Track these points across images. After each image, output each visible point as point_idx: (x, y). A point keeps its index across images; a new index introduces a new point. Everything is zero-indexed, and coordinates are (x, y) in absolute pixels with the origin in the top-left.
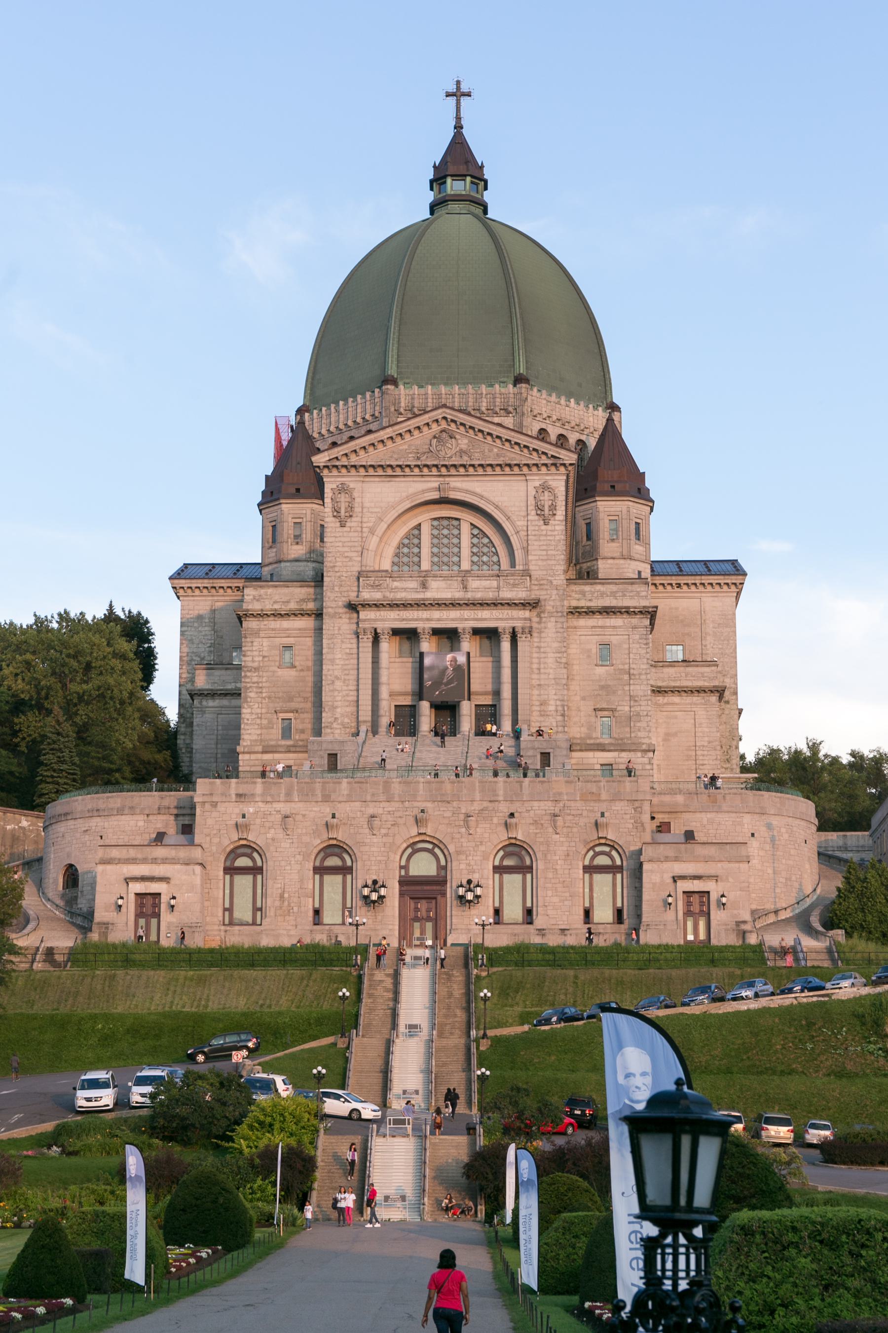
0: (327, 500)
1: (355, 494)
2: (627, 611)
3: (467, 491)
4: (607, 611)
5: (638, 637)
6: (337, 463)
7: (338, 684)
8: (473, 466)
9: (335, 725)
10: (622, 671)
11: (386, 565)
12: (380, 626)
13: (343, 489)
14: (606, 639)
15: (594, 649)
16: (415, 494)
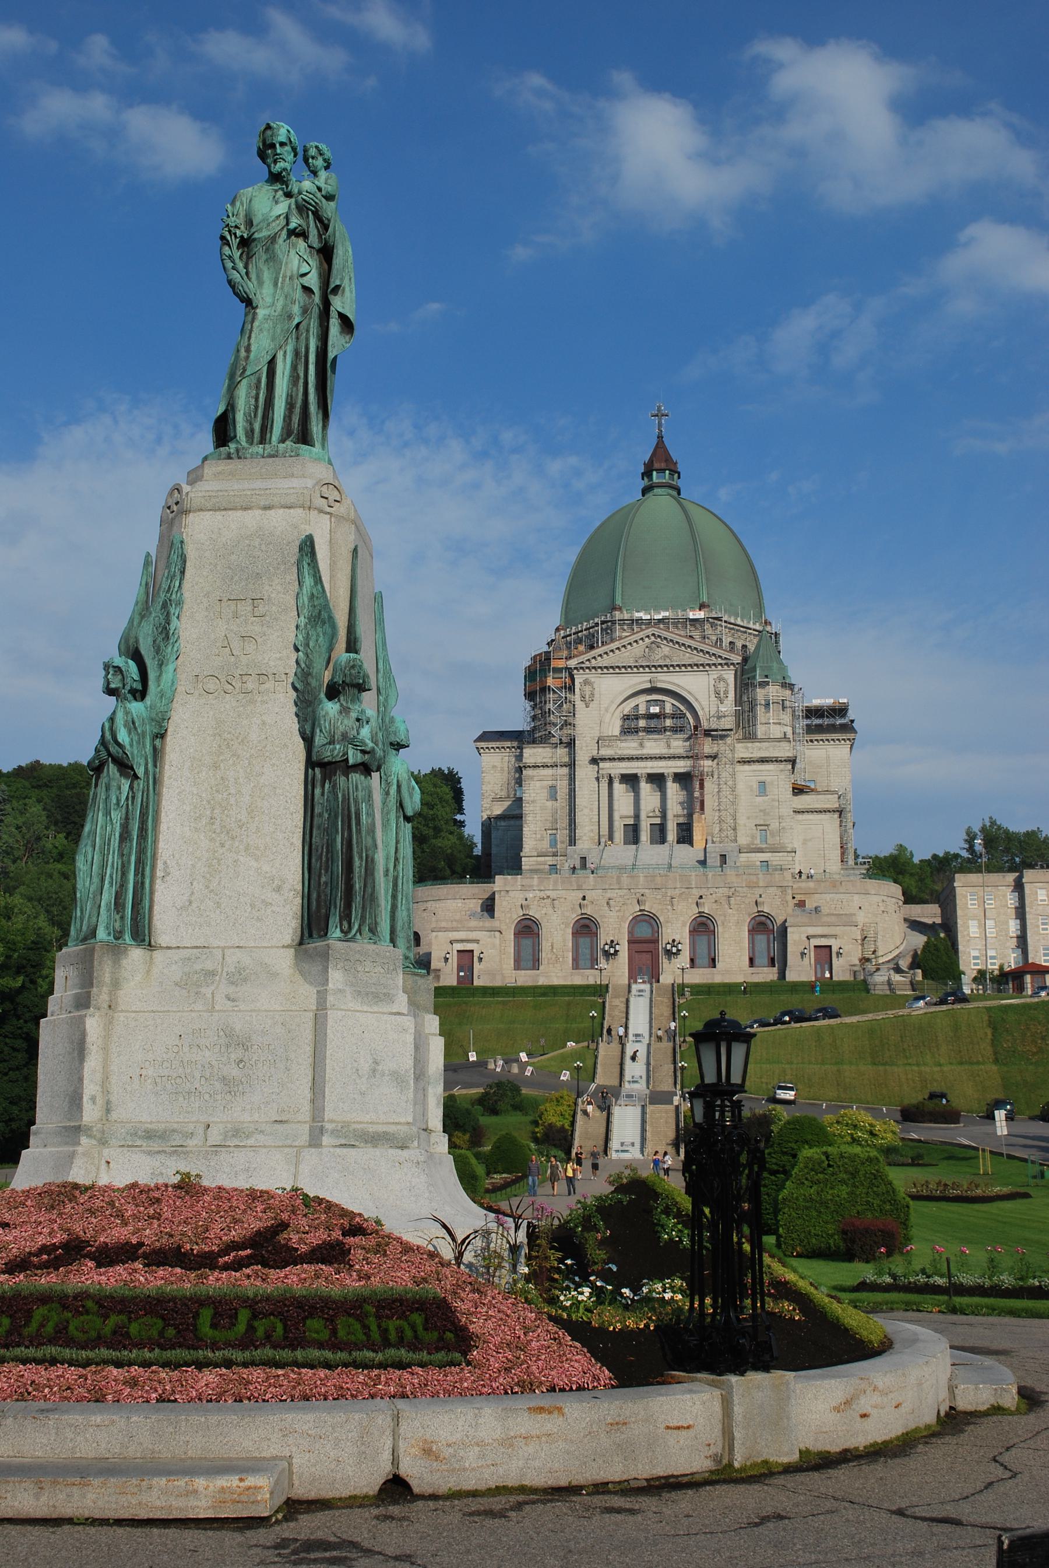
0: (577, 690)
1: (595, 686)
2: (777, 760)
3: (669, 683)
4: (763, 761)
5: (783, 777)
6: (583, 665)
7: (586, 811)
8: (672, 666)
9: (584, 838)
10: (773, 800)
11: (617, 731)
12: (613, 772)
13: (586, 682)
14: (762, 779)
15: (755, 786)
16: (635, 685)
